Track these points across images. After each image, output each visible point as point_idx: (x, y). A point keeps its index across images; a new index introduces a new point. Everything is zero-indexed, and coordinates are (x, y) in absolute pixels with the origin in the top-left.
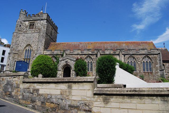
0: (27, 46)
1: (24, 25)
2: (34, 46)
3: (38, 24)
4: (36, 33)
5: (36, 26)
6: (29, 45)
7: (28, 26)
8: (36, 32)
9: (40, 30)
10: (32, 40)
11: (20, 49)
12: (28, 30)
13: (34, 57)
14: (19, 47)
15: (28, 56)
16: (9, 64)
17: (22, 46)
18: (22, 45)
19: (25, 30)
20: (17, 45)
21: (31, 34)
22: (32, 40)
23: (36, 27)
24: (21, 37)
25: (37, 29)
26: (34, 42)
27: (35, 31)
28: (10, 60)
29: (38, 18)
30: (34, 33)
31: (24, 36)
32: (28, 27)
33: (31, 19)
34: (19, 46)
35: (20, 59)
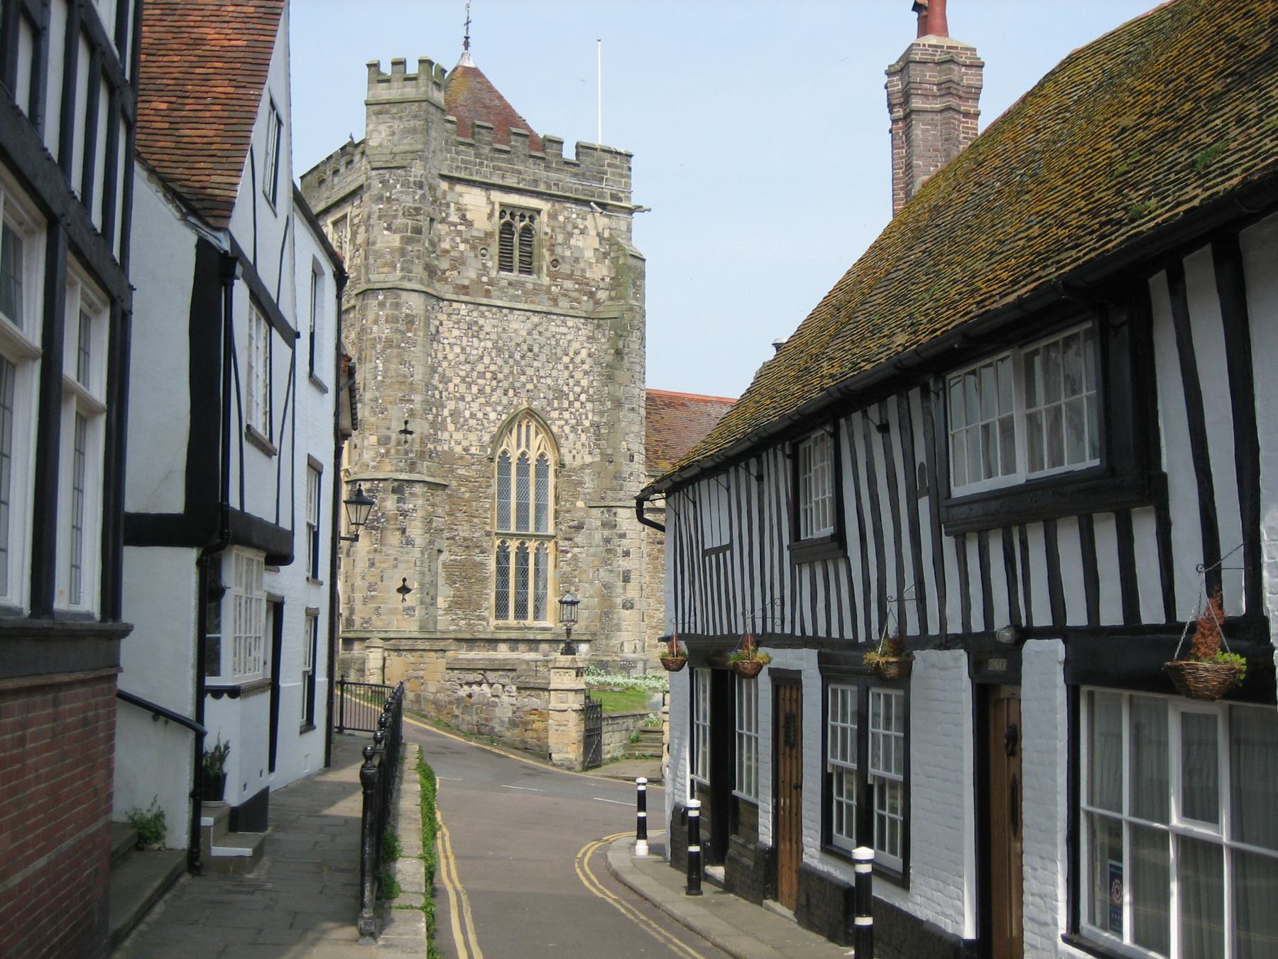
0: (507, 427)
1: (454, 218)
2: (567, 429)
3: (571, 235)
4: (570, 322)
5: (559, 250)
6: (530, 413)
7: (489, 235)
8: (564, 305)
9: (592, 295)
10: (549, 381)
11: (458, 449)
12: (493, 274)
13: (579, 527)
14: (451, 427)
15: (522, 508)
16: (414, 584)
17: (473, 422)
18: (473, 416)
19: (472, 274)
20: (434, 410)
21: (536, 319)
22: (549, 381)
23: (555, 263)
24: (451, 333)
25: (568, 284)
26: (561, 394)
27: (555, 301)
28: (409, 542)
29: (569, 184)
30: (559, 320)
31: (473, 330)
32: (495, 248)
33: (511, 181)
34: (444, 420)
35: (466, 534)
